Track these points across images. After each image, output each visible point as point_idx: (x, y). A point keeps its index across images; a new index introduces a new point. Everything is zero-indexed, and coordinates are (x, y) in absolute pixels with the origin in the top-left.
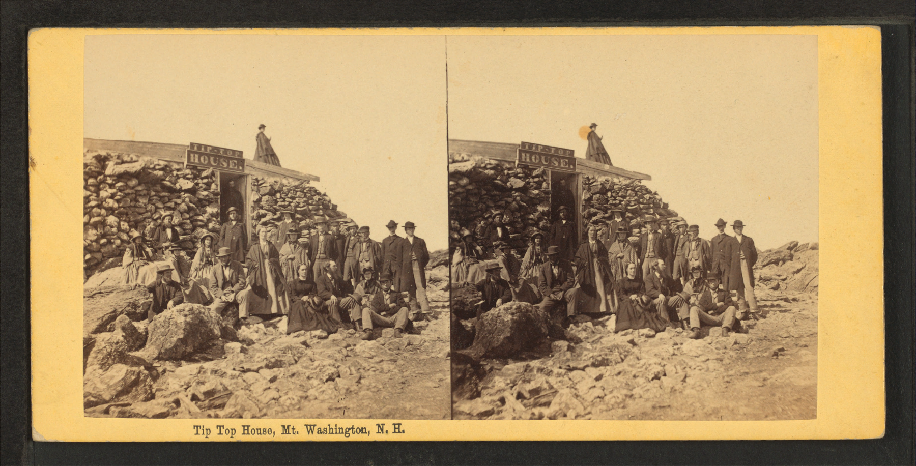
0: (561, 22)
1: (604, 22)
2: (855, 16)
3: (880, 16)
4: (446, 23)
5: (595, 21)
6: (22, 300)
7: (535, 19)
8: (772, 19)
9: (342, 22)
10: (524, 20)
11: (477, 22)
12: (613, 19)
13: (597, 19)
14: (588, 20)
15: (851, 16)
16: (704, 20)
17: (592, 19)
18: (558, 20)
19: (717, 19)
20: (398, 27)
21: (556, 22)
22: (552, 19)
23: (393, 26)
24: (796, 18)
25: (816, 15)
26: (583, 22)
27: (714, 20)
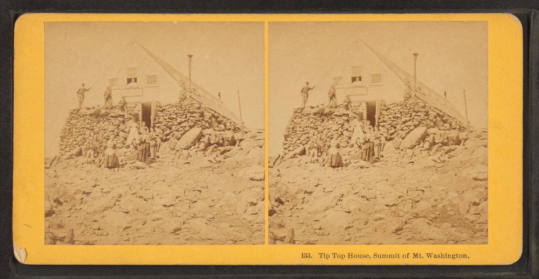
0: (325, 11)
1: (350, 11)
2: (496, 8)
3: (511, 8)
4: (258, 11)
5: (345, 11)
6: (10, 171)
7: (310, 9)
8: (447, 9)
9: (197, 10)
10: (303, 10)
11: (276, 11)
12: (355, 9)
13: (346, 9)
14: (341, 10)
15: (494, 8)
16: (408, 10)
17: (343, 9)
18: (324, 9)
19: (416, 9)
20: (230, 13)
21: (322, 11)
22: (320, 9)
23: (227, 13)
24: (462, 9)
25: (473, 8)
26: (338, 11)
27: (414, 10)
